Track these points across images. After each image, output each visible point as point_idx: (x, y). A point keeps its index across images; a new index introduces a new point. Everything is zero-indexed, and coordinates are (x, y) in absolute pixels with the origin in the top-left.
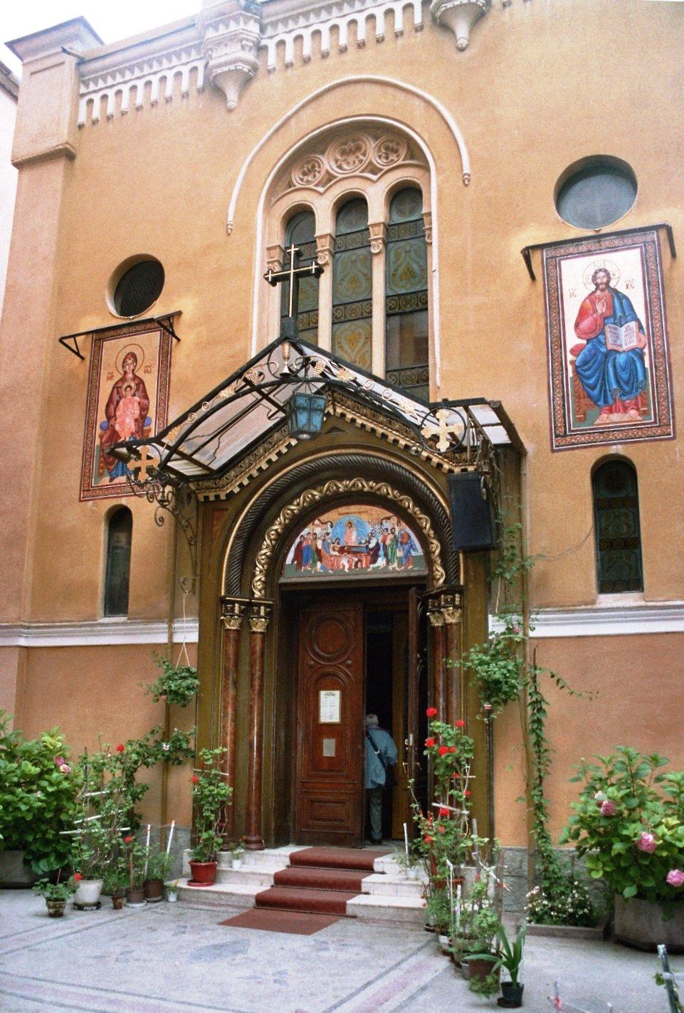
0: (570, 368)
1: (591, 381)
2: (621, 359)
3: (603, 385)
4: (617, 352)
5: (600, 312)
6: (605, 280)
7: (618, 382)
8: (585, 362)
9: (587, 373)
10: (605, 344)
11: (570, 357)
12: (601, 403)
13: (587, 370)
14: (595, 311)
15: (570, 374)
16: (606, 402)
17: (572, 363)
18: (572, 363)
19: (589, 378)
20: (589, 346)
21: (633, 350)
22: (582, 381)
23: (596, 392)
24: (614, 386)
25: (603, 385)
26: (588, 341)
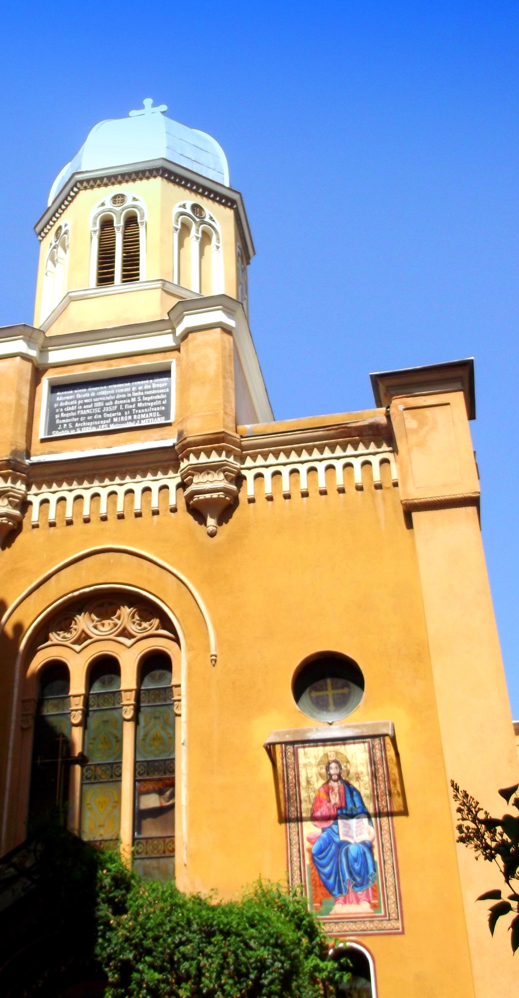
0: (307, 855)
1: (327, 870)
2: (353, 851)
3: (337, 874)
4: (347, 843)
5: (333, 802)
6: (337, 771)
7: (351, 874)
8: (321, 851)
9: (324, 862)
10: (338, 834)
11: (307, 844)
12: (336, 892)
13: (323, 858)
14: (329, 801)
15: (308, 861)
16: (340, 892)
17: (309, 850)
18: (309, 850)
19: (324, 866)
20: (324, 835)
21: (364, 843)
22: (319, 871)
23: (331, 881)
24: (347, 876)
25: (337, 874)
26: (323, 830)
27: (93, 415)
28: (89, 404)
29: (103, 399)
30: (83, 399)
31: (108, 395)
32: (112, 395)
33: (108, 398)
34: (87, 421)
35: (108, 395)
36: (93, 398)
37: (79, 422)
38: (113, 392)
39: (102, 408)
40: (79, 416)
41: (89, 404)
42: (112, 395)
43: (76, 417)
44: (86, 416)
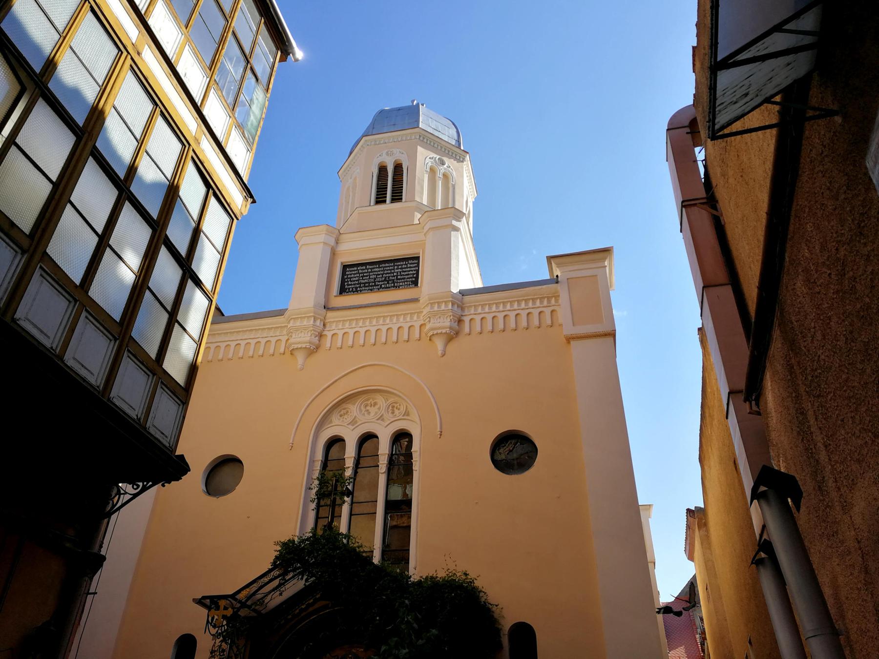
27: (369, 283)
28: (367, 276)
29: (376, 273)
30: (363, 273)
31: (379, 271)
32: (382, 271)
33: (379, 273)
34: (365, 286)
35: (379, 271)
36: (370, 272)
37: (360, 287)
38: (382, 269)
39: (375, 279)
40: (361, 283)
41: (367, 276)
42: (382, 271)
43: (358, 284)
44: (365, 283)
